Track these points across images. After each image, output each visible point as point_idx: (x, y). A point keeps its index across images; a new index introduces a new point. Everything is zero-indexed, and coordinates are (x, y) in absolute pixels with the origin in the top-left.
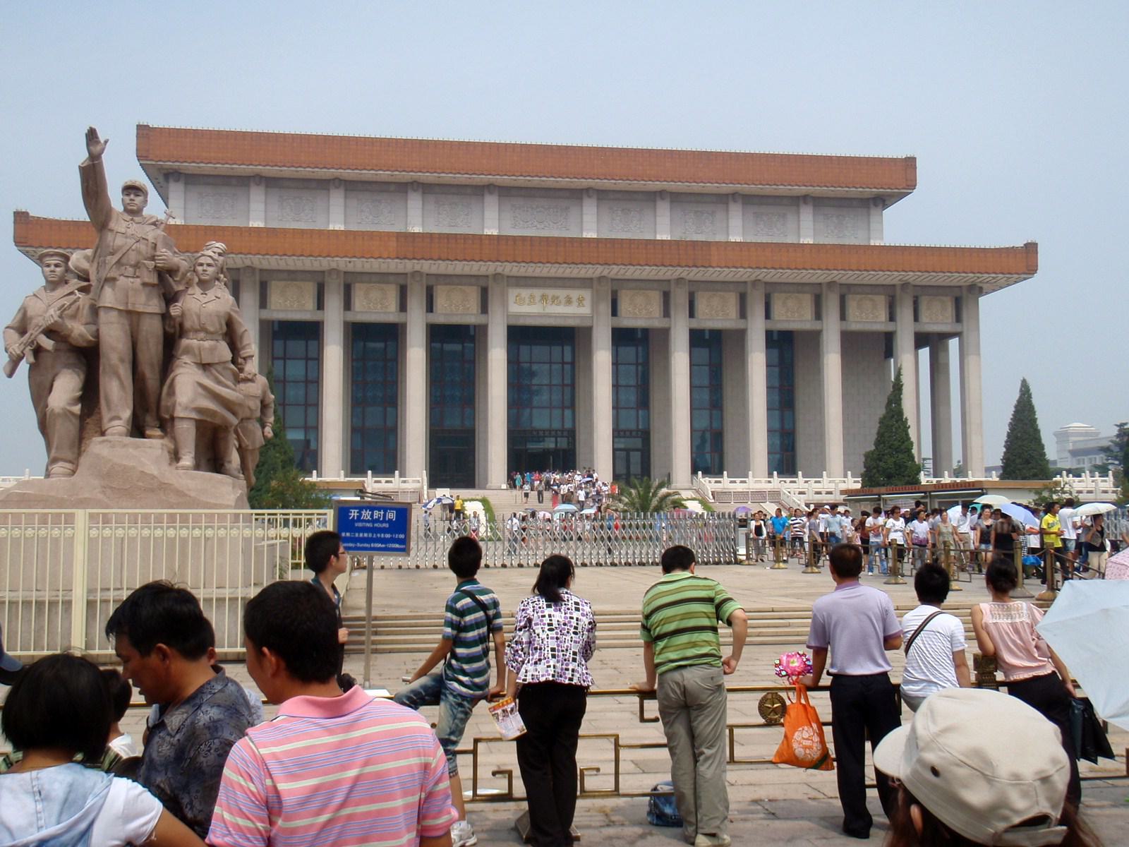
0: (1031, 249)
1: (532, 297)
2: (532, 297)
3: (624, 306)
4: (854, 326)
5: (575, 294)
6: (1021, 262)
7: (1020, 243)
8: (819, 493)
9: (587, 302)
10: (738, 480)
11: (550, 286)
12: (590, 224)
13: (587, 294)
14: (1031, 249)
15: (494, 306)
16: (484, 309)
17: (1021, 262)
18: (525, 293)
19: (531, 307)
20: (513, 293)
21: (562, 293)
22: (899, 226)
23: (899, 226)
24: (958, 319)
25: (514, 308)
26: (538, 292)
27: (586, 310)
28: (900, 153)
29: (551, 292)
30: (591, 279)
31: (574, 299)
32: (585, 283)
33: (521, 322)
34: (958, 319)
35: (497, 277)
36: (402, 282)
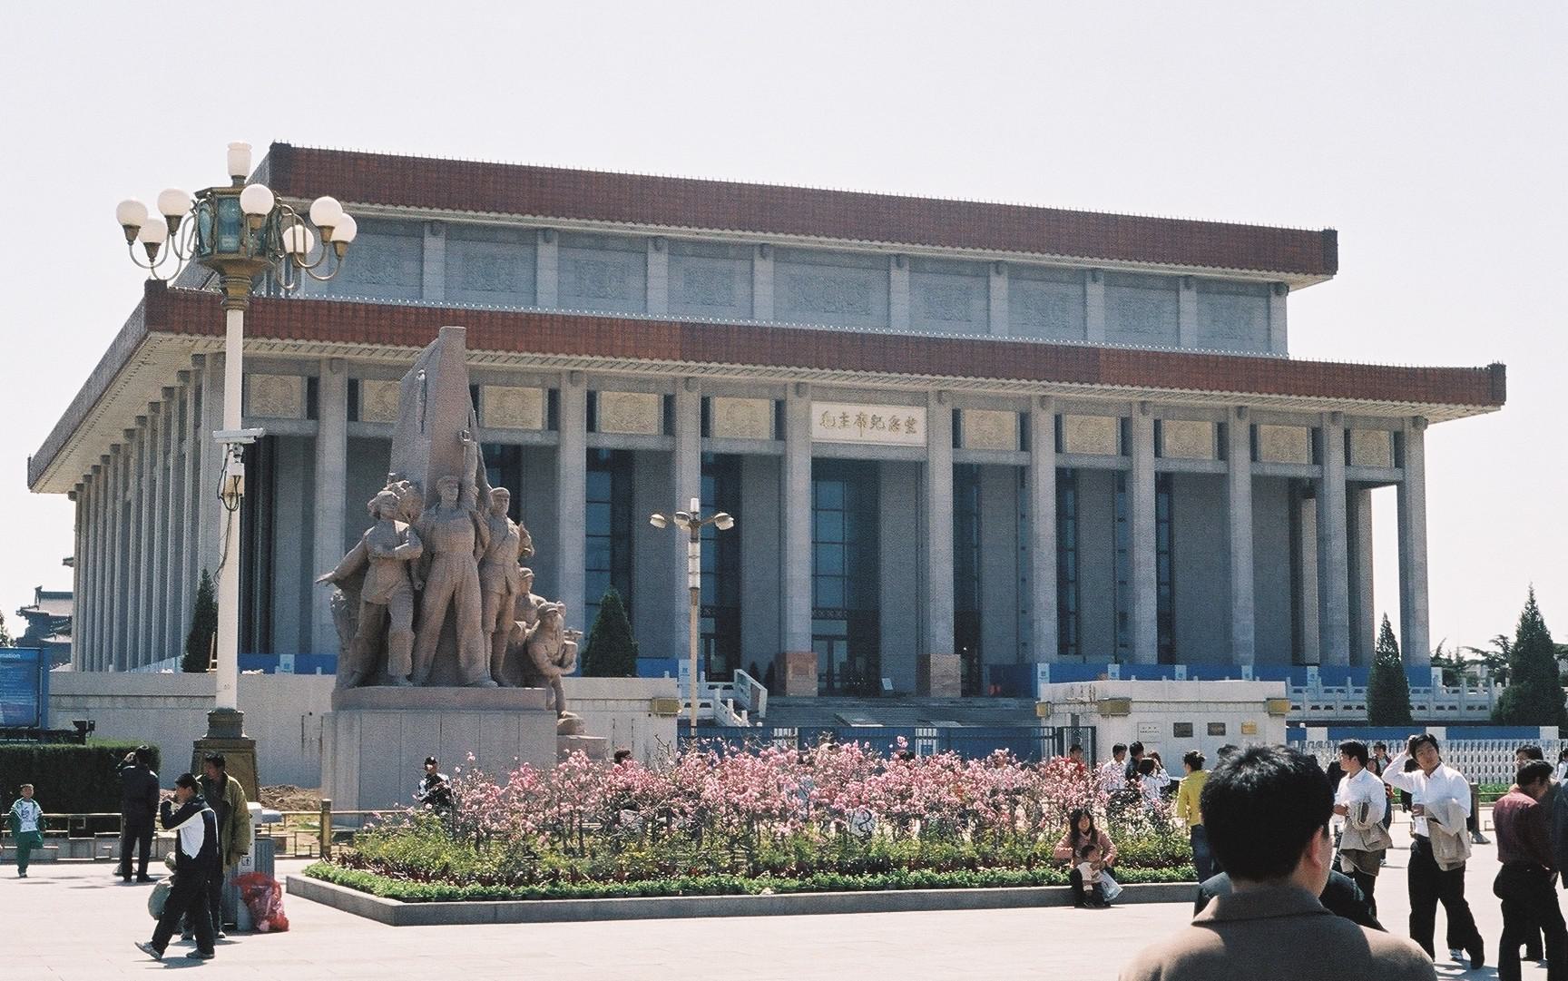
0: (1497, 371)
1: (844, 417)
2: (844, 417)
3: (605, 413)
4: (1268, 471)
5: (903, 413)
6: (1482, 388)
7: (1483, 363)
8: (1441, 708)
9: (920, 427)
10: (1335, 688)
13: (919, 414)
14: (1497, 371)
15: (794, 431)
17: (1482, 388)
18: (836, 409)
20: (818, 409)
21: (886, 412)
22: (1316, 325)
23: (1316, 325)
24: (1399, 462)
25: (820, 432)
27: (919, 438)
28: (1318, 227)
29: (870, 411)
32: (919, 399)
33: (829, 453)
34: (1399, 462)
35: (798, 387)
36: (780, 395)
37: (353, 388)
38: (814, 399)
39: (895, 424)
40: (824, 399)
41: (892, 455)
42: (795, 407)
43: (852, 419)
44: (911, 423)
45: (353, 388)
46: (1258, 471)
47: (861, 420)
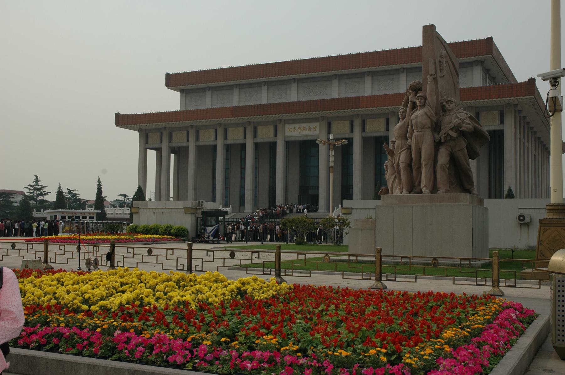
5: (312, 125)
9: (318, 129)
11: (302, 123)
12: (335, 92)
13: (317, 125)
16: (276, 136)
18: (292, 126)
19: (297, 132)
20: (287, 126)
21: (307, 125)
26: (297, 126)
27: (317, 132)
30: (319, 118)
31: (312, 128)
32: (316, 120)
33: (290, 139)
35: (280, 121)
37: (197, 133)
38: (285, 123)
39: (310, 128)
40: (289, 123)
41: (293, 139)
42: (279, 128)
43: (312, 128)
44: (315, 128)
45: (197, 133)
46: (365, 135)
47: (300, 128)
